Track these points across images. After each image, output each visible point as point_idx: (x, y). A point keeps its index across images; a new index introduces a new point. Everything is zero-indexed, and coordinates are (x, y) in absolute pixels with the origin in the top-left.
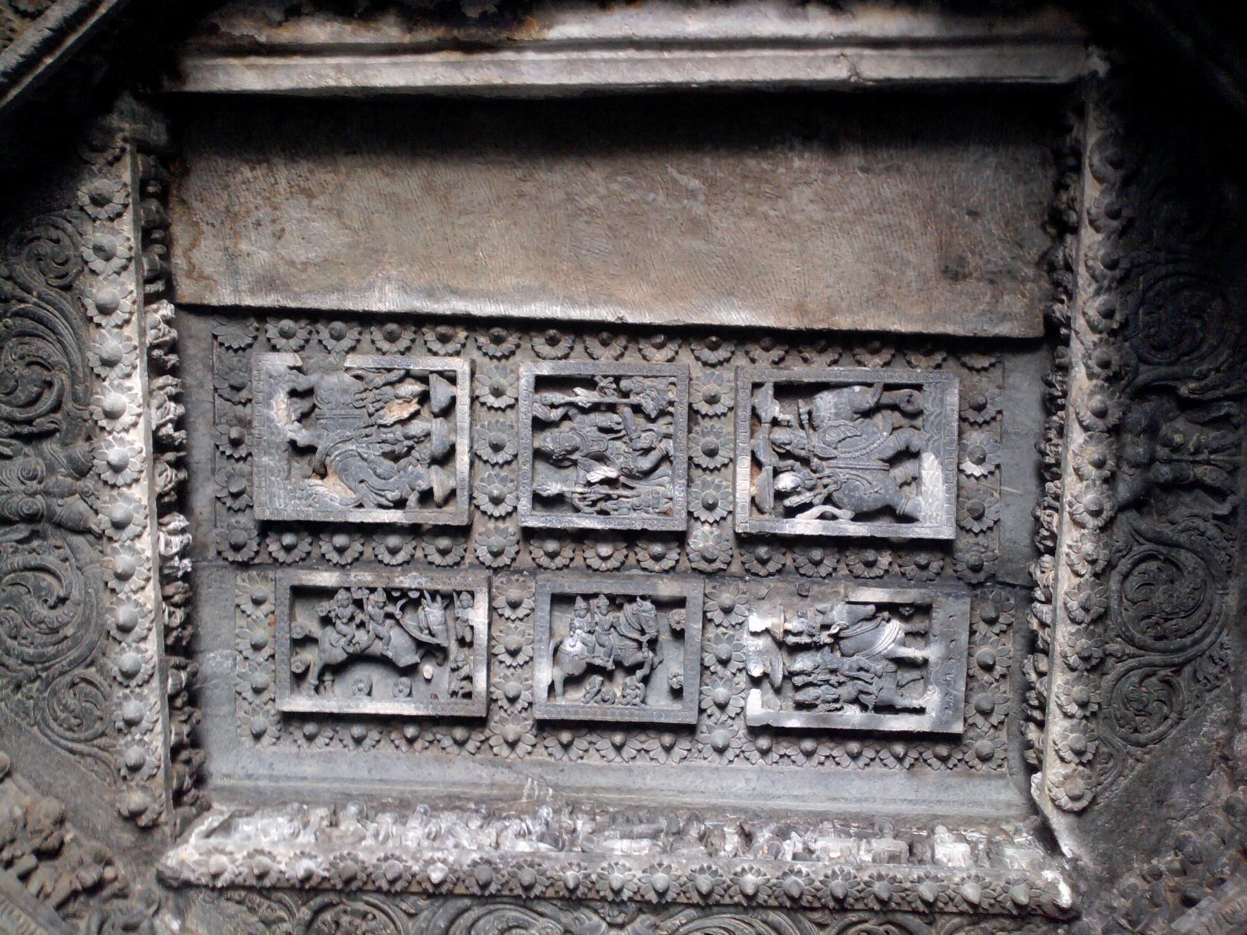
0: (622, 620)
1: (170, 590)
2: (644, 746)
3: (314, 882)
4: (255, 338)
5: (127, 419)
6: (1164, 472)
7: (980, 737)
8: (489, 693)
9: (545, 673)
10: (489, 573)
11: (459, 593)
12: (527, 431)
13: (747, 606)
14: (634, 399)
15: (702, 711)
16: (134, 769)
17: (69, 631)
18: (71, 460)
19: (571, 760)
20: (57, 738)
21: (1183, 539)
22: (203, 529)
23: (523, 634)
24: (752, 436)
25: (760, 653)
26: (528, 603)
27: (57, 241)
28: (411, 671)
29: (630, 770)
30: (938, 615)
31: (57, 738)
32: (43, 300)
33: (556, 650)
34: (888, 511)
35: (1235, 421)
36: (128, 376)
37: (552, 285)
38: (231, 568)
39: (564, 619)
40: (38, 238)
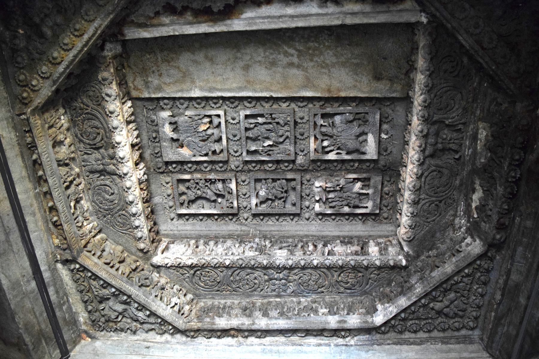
0: (277, 185)
1: (142, 186)
3: (194, 265)
4: (157, 106)
5: (123, 144)
6: (440, 146)
8: (238, 206)
9: (254, 201)
10: (235, 173)
11: (227, 180)
12: (243, 132)
14: (276, 120)
15: (301, 209)
16: (141, 238)
17: (116, 202)
18: (109, 155)
22: (149, 163)
23: (247, 189)
24: (315, 130)
25: (318, 192)
26: (248, 180)
27: (94, 91)
28: (215, 201)
29: (281, 225)
30: (372, 182)
33: (257, 193)
34: (357, 151)
35: (462, 130)
36: (121, 131)
37: (249, 86)
39: (259, 185)
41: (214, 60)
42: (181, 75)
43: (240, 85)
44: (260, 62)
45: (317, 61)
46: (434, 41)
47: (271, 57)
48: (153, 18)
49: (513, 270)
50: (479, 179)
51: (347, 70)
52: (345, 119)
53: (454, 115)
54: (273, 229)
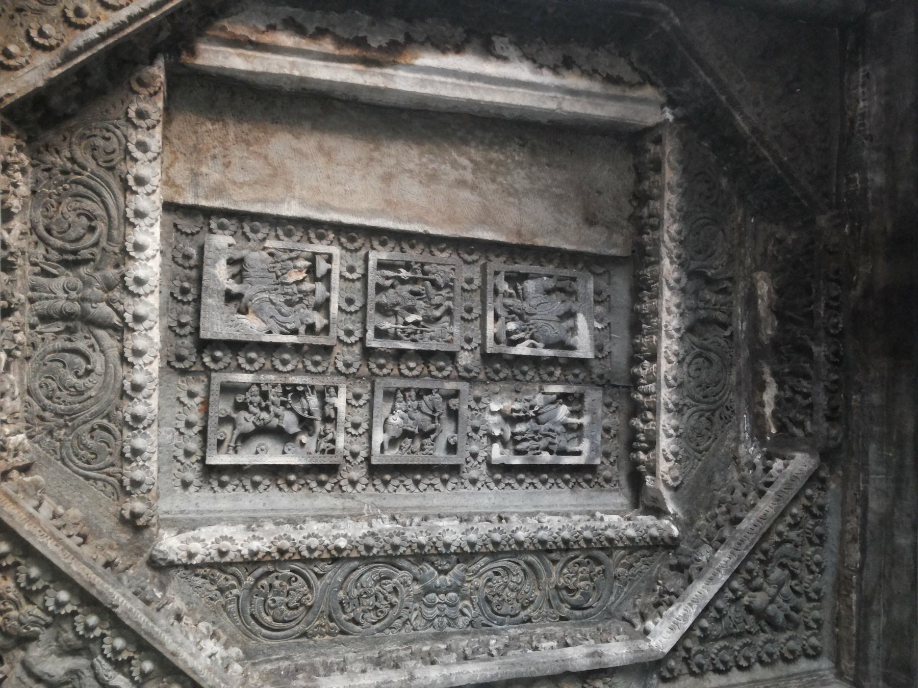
5: (149, 252)
7: (605, 469)
14: (431, 277)
17: (93, 393)
20: (76, 468)
21: (712, 347)
23: (362, 415)
27: (108, 139)
30: (587, 401)
31: (76, 468)
32: (95, 174)
34: (562, 345)
37: (388, 210)
40: (95, 136)
42: (268, 171)
44: (411, 171)
45: (501, 184)
46: (685, 145)
47: (431, 166)
48: (263, 32)
49: (871, 489)
50: (768, 364)
52: (543, 285)
53: (717, 263)
54: (408, 503)
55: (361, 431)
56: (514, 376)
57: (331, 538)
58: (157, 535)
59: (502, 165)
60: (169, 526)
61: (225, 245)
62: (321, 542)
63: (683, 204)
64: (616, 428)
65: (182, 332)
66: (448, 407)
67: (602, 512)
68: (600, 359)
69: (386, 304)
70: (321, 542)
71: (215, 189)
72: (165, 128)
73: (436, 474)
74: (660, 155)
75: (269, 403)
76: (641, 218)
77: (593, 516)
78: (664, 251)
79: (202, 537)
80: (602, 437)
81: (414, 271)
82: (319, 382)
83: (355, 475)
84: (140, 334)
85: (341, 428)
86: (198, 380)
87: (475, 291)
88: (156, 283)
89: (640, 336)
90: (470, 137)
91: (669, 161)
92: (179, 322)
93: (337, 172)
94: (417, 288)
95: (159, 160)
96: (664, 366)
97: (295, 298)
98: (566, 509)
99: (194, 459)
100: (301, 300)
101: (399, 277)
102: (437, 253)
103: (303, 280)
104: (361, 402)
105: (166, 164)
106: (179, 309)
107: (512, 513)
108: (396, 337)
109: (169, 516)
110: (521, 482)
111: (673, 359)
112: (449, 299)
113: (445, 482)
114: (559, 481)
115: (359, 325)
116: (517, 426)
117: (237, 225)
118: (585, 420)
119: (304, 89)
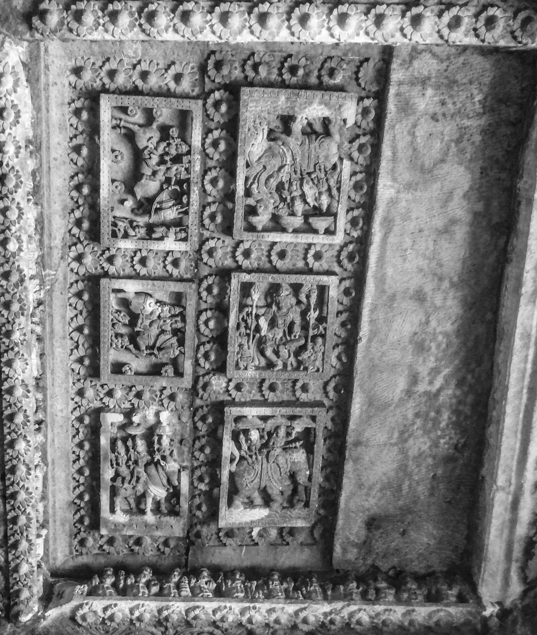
2: (81, 346)
7: (95, 540)
13: (174, 409)
19: (69, 299)
23: (155, 268)
34: (234, 491)
37: (385, 298)
38: (202, 60)
41: (446, 236)
42: (427, 163)
43: (389, 281)
44: (427, 322)
45: (413, 424)
47: (433, 345)
51: (392, 474)
52: (300, 470)
54: (57, 319)
55: (138, 267)
56: (198, 438)
57: (18, 234)
58: (22, 39)
59: (434, 424)
60: (31, 53)
61: (345, 116)
62: (13, 223)
63: (391, 627)
64: (141, 552)
65: (247, 68)
66: (164, 365)
67: (47, 536)
68: (218, 534)
69: (279, 296)
70: (13, 223)
71: (407, 104)
72: (476, 48)
73: (89, 351)
74: (445, 601)
75: (169, 164)
76: (376, 580)
77: (43, 526)
78: (339, 605)
79: (19, 89)
80: (131, 536)
81: (316, 327)
82: (192, 220)
83: (88, 260)
84: (245, 20)
85: (140, 245)
86: (194, 86)
87: (294, 395)
88: (303, 39)
89: (243, 578)
90: (466, 389)
91: (438, 611)
92: (260, 64)
93: (427, 241)
94: (297, 329)
95: (440, 41)
96: (210, 606)
97: (286, 194)
98: (50, 496)
99: (106, 80)
100: (283, 200)
101: (309, 310)
102: (337, 351)
103: (305, 202)
104: (170, 268)
105: (436, 49)
106: (274, 64)
107: (46, 436)
108: (242, 307)
109: (42, 53)
110: (80, 445)
111: (218, 616)
112: (285, 365)
113: (80, 361)
114: (82, 488)
115: (255, 265)
116: (143, 442)
117: (368, 129)
118: (150, 517)
119: (519, 203)
